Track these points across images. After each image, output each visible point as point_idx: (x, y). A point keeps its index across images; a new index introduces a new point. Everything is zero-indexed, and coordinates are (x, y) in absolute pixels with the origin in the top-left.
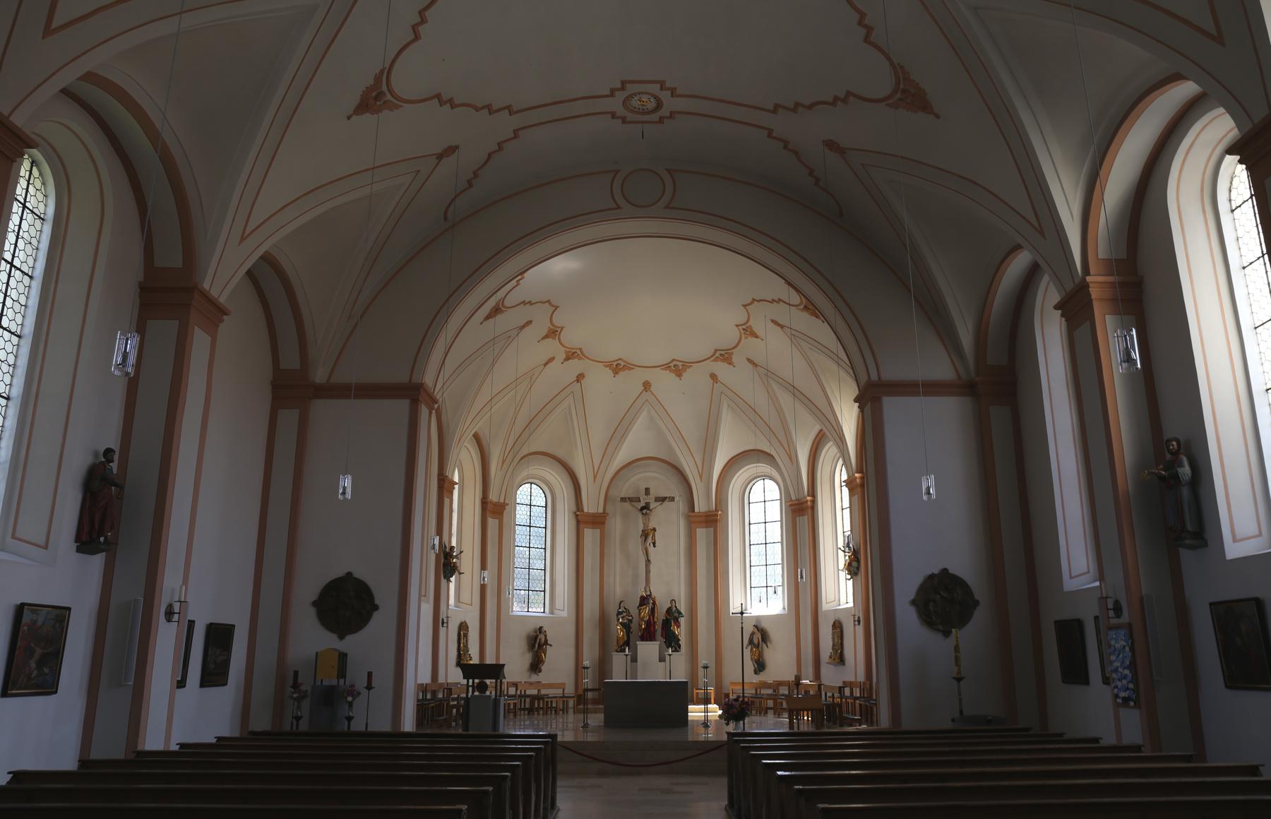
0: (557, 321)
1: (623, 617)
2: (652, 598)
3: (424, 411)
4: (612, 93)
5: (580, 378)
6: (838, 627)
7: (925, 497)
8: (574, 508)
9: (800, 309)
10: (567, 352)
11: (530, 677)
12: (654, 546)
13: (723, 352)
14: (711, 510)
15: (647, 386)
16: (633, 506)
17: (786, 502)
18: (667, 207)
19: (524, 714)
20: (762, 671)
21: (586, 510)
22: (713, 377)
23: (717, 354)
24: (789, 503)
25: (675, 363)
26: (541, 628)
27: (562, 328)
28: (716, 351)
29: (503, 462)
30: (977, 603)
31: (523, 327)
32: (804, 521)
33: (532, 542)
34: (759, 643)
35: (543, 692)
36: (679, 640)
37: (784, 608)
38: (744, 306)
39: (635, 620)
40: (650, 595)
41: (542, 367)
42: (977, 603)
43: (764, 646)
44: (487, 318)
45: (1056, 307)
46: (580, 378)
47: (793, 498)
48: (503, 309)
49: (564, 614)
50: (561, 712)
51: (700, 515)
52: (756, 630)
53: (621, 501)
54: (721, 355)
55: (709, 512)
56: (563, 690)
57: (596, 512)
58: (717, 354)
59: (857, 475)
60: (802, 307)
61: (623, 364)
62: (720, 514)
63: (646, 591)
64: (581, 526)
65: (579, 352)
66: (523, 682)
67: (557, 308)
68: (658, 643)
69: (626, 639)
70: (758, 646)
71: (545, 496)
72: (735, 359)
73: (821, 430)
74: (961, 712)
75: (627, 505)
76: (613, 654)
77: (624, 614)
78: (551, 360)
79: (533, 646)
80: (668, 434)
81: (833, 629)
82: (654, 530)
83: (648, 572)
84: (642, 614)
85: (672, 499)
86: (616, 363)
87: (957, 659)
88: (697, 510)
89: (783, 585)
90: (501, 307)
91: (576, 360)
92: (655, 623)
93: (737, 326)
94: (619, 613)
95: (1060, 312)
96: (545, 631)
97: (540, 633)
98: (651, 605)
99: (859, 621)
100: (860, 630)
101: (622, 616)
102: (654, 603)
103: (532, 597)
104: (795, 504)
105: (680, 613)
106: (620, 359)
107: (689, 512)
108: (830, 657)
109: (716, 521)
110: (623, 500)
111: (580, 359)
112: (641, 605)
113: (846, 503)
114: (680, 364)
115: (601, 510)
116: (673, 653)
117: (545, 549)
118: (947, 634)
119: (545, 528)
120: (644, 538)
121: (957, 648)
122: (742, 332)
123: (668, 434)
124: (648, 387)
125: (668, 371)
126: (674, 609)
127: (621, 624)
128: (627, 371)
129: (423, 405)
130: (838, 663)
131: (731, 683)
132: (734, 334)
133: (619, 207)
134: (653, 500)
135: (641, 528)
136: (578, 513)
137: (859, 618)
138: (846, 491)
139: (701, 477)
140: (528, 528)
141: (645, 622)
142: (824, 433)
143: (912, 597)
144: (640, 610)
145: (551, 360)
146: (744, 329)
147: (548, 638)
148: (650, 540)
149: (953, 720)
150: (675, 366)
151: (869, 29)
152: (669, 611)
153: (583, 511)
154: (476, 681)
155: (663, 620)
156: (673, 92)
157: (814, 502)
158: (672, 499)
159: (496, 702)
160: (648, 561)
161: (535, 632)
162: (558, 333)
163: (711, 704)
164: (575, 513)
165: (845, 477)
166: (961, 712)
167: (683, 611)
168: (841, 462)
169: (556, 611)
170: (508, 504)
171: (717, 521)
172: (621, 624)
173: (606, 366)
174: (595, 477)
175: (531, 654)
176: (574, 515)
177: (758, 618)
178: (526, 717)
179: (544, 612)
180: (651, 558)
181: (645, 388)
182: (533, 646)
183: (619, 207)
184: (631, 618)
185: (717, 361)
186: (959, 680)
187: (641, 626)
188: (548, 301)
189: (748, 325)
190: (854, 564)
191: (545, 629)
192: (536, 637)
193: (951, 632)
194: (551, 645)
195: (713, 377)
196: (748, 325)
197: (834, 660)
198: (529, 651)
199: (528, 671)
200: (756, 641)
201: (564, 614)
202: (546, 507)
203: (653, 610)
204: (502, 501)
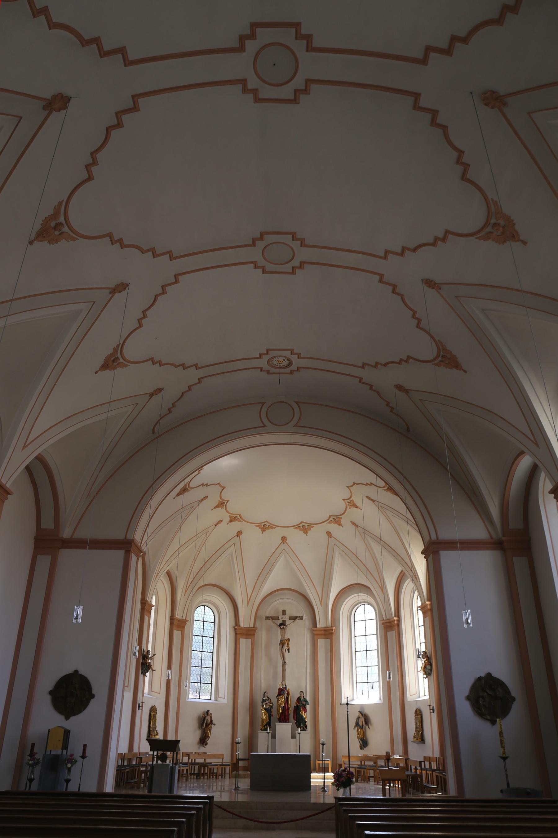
0: (225, 496)
1: (266, 704)
2: (287, 690)
3: (133, 558)
4: (261, 356)
5: (239, 534)
6: (419, 713)
7: (465, 626)
8: (233, 624)
9: (384, 490)
10: (231, 517)
11: (199, 748)
12: (289, 652)
13: (335, 517)
15: (284, 539)
16: (274, 623)
17: (380, 621)
18: (295, 426)
19: (194, 779)
20: (365, 747)
21: (241, 625)
22: (329, 534)
23: (331, 519)
24: (382, 622)
25: (303, 524)
26: (208, 711)
27: (228, 501)
28: (330, 516)
29: (186, 591)
30: (513, 699)
31: (202, 500)
32: (392, 635)
33: (204, 647)
34: (363, 726)
35: (208, 761)
36: (306, 722)
37: (380, 699)
38: (348, 487)
39: (275, 706)
40: (285, 688)
41: (214, 526)
42: (513, 699)
43: (367, 727)
44: (178, 495)
45: (551, 492)
46: (239, 534)
47: (385, 618)
48: (189, 489)
49: (225, 701)
50: (220, 777)
51: (321, 630)
52: (361, 715)
53: (266, 620)
54: (333, 519)
55: (327, 627)
56: (222, 759)
58: (331, 519)
59: (427, 603)
60: (386, 488)
61: (268, 524)
63: (282, 685)
64: (238, 636)
65: (239, 517)
66: (194, 753)
67: (224, 488)
68: (291, 724)
69: (268, 720)
70: (363, 728)
71: (214, 615)
72: (343, 522)
73: (402, 571)
74: (508, 785)
75: (270, 622)
76: (259, 731)
77: (267, 702)
78: (221, 521)
79: (202, 724)
80: (298, 573)
81: (415, 716)
82: (289, 640)
83: (284, 670)
84: (280, 702)
85: (301, 618)
86: (262, 524)
87: (502, 742)
88: (318, 626)
89: (379, 682)
90: (188, 488)
91: (237, 522)
92: (289, 708)
93: (344, 500)
94: (264, 701)
95: (553, 495)
96: (211, 714)
97: (207, 715)
98: (286, 695)
99: (433, 710)
100: (434, 716)
101: (265, 703)
102: (288, 694)
103: (202, 688)
104: (386, 623)
105: (306, 701)
106: (266, 521)
107: (313, 627)
108: (414, 737)
109: (332, 634)
110: (267, 618)
111: (239, 521)
113: (421, 623)
114: (306, 525)
115: (252, 626)
116: (302, 732)
117: (213, 653)
118: (493, 722)
119: (213, 638)
120: (281, 646)
121: (501, 734)
122: (348, 504)
123: (298, 573)
124: (285, 540)
125: (298, 530)
126: (302, 698)
127: (265, 709)
128: (271, 529)
129: (133, 554)
130: (420, 741)
131: (342, 756)
132: (343, 505)
133: (265, 426)
134: (288, 618)
135: (280, 639)
136: (236, 627)
137: (433, 707)
138: (420, 613)
139: (321, 602)
140: (202, 637)
141: (282, 707)
142: (405, 573)
143: (467, 693)
144: (278, 699)
145: (221, 521)
146: (348, 502)
147: (213, 719)
148: (285, 647)
149: (502, 791)
150: (303, 526)
151: (419, 320)
152: (299, 699)
153: (239, 626)
154: (160, 752)
155: (295, 706)
156: (299, 356)
157: (399, 621)
158: (301, 618)
159: (173, 769)
160: (284, 663)
161: (204, 714)
162: (225, 504)
163: (328, 772)
164: (234, 627)
165: (420, 604)
166: (508, 785)
167: (308, 700)
168: (416, 593)
169: (219, 699)
170: (188, 621)
171: (332, 634)
172: (265, 709)
173: (257, 526)
174: (248, 602)
175: (200, 730)
176: (234, 629)
177: (362, 706)
178: (195, 780)
179: (211, 699)
180: (286, 661)
181: (283, 541)
182: (202, 724)
183: (265, 426)
184: (271, 705)
185: (331, 523)
186: (504, 759)
187: (278, 711)
188: (219, 484)
189: (351, 500)
190: (428, 667)
191: (210, 712)
192: (205, 718)
193: (496, 721)
194: (214, 725)
195: (329, 534)
196: (351, 500)
197: (417, 739)
198: (199, 730)
199: (198, 744)
200: (361, 724)
201: (225, 701)
202: (214, 623)
203: (287, 699)
204: (184, 618)
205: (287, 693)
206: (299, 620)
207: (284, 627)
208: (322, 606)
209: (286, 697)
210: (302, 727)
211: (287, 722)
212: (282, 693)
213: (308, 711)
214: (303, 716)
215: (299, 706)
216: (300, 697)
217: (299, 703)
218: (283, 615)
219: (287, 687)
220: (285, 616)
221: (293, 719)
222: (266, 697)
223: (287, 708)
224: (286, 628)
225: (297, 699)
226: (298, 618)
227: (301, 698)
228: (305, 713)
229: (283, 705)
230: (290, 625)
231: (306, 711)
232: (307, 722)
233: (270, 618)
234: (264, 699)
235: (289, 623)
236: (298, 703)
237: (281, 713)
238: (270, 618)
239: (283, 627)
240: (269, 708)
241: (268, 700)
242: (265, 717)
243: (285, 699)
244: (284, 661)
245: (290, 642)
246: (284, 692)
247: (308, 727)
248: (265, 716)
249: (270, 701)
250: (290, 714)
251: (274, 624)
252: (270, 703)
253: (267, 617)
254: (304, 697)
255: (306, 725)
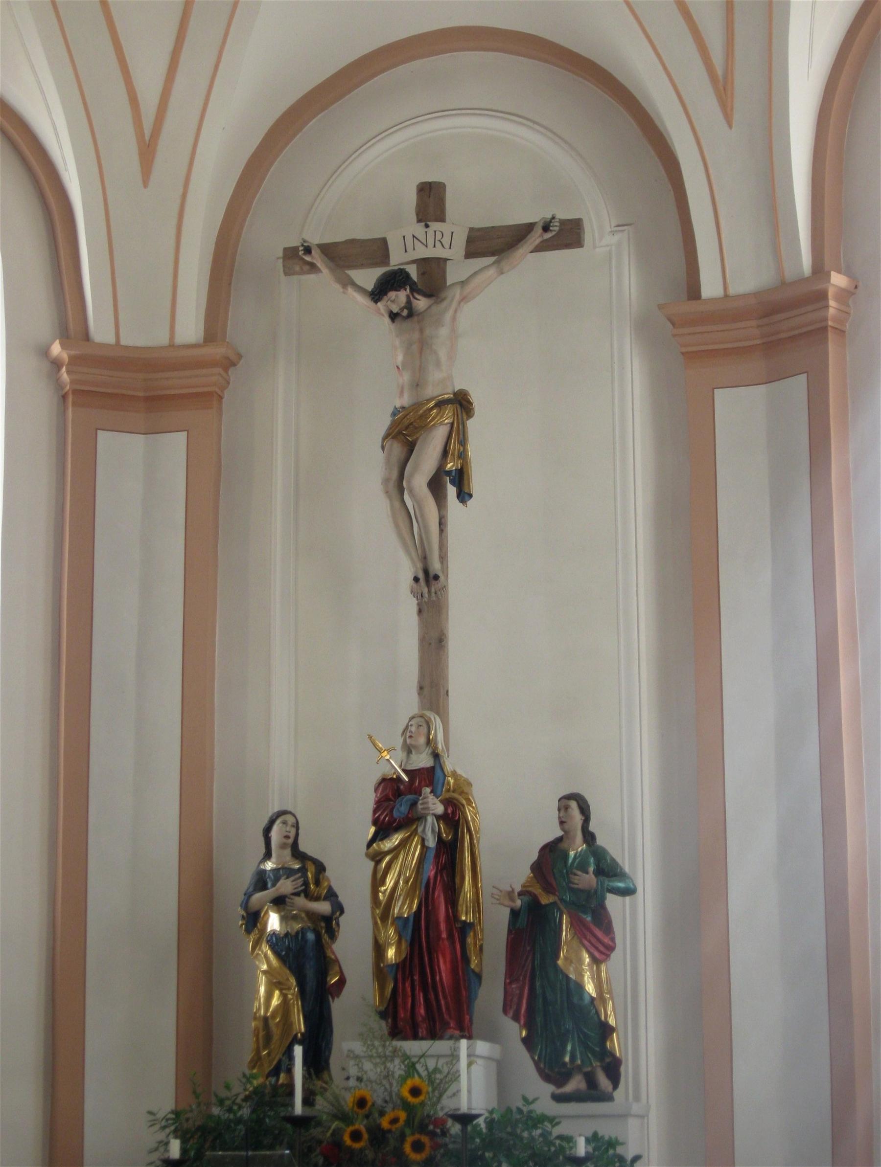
1: (279, 902)
14: (790, 275)
55: (783, 284)
57: (160, 338)
62: (845, 295)
63: (409, 750)
84: (390, 882)
101: (270, 893)
112: (383, 830)
120: (397, 449)
126: (577, 848)
141: (401, 923)
164: (45, 352)
171: (824, 329)
184: (324, 907)
187: (379, 950)
205: (440, 809)
206: (538, 249)
207: (421, 303)
208: (737, 117)
209: (440, 840)
210: (579, 1069)
211: (449, 1032)
212: (401, 809)
213: (618, 940)
214: (580, 987)
215: (554, 903)
216: (560, 840)
217: (549, 888)
218: (419, 221)
219: (449, 766)
220: (435, 226)
221: (505, 1011)
222: (288, 852)
223: (443, 926)
224: (435, 309)
225: (534, 856)
226: (536, 237)
227: (564, 845)
228: (595, 961)
229: (403, 908)
230: (468, 289)
231: (611, 949)
232: (612, 1030)
233: (316, 252)
234: (269, 866)
235: (463, 279)
236: (538, 891)
237: (403, 967)
238: (316, 252)
239: (409, 305)
240: (311, 936)
241: (303, 870)
242: (275, 1001)
243: (431, 855)
244: (426, 572)
245: (471, 424)
246: (414, 804)
247: (622, 1069)
248: (277, 993)
249: (317, 883)
250: (479, 977)
251: (344, 286)
252: (317, 899)
253: (295, 249)
254: (589, 837)
255: (613, 1055)
